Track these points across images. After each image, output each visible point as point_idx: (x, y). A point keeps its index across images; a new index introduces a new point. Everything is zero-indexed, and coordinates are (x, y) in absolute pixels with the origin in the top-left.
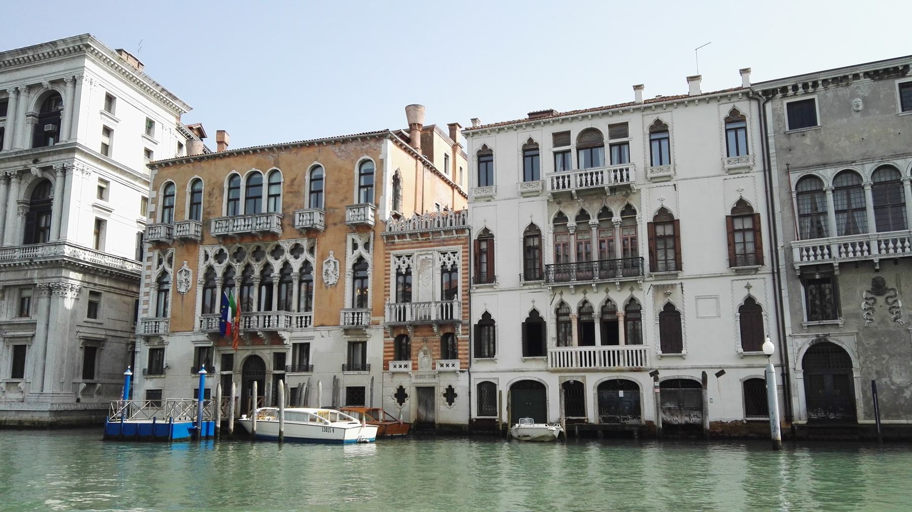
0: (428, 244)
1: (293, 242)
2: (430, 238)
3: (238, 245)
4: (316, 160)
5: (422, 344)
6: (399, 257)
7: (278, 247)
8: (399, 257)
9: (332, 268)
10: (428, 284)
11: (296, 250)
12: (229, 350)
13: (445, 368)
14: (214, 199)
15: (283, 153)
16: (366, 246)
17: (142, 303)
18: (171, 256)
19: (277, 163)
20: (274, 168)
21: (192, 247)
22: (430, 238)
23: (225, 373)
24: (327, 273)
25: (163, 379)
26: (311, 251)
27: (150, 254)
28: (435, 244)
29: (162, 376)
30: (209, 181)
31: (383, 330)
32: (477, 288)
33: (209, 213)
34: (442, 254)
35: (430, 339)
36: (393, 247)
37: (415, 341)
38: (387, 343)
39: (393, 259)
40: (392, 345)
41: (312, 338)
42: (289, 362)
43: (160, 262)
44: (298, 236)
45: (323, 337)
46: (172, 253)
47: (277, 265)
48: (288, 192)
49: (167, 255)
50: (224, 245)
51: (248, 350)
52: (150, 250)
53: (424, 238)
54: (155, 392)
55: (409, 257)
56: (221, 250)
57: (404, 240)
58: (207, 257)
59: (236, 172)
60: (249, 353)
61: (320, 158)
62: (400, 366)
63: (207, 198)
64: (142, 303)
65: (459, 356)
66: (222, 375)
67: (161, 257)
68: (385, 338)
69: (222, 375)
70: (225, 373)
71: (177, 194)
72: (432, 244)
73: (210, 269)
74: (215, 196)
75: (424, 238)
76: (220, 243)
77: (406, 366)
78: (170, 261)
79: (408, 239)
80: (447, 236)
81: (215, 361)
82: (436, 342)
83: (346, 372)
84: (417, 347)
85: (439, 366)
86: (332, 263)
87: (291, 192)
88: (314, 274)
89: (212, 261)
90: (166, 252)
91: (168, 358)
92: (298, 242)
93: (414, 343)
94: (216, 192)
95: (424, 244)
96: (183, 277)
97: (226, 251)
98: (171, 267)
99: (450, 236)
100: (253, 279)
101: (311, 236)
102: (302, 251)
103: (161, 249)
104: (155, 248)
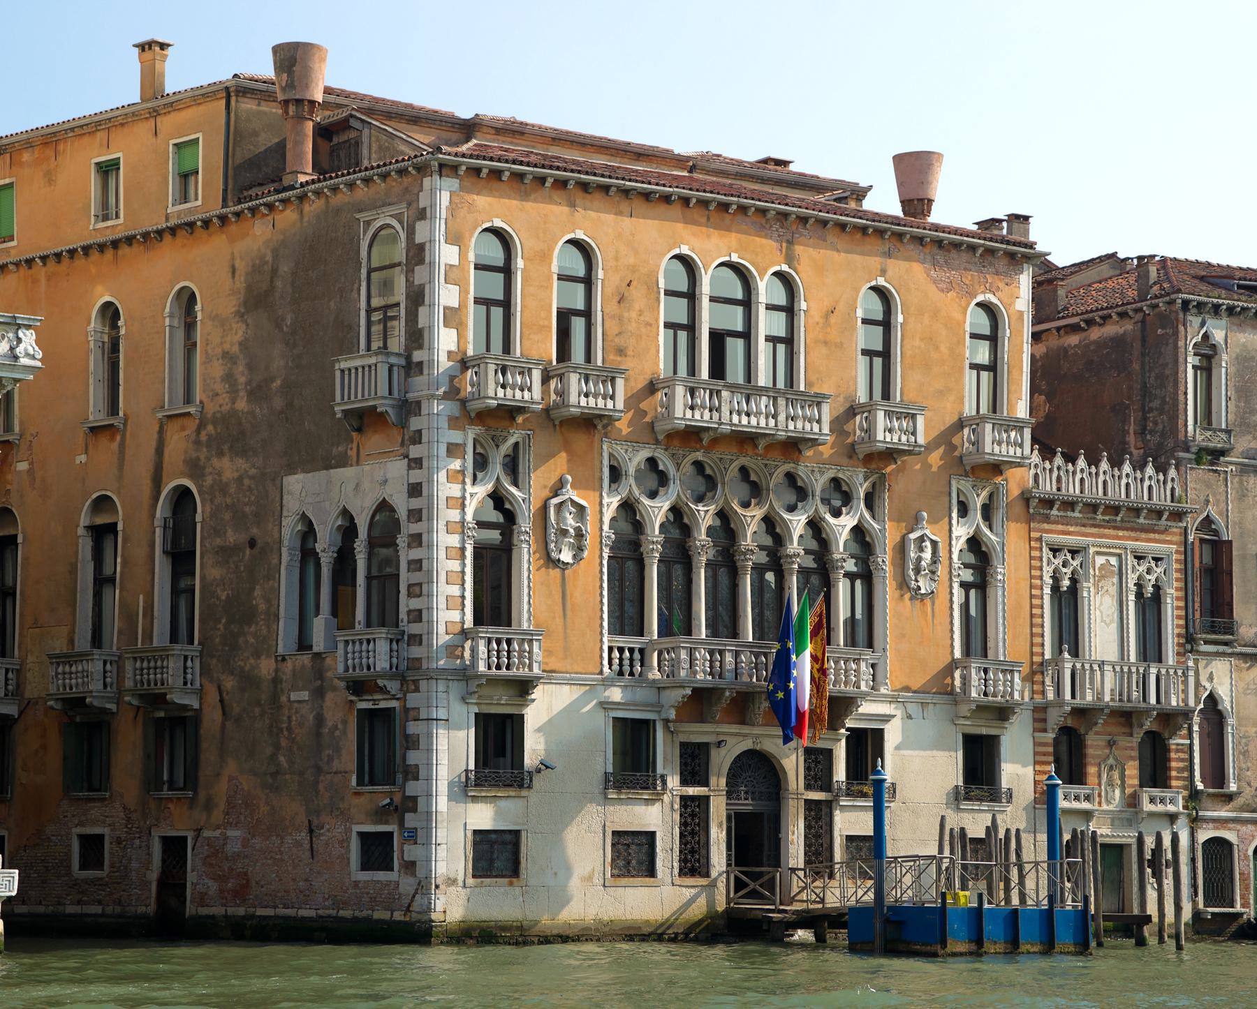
0: (1112, 532)
1: (831, 474)
2: (1119, 518)
3: (699, 456)
4: (883, 272)
5: (1107, 751)
6: (1055, 551)
7: (791, 478)
8: (1055, 551)
9: (927, 555)
10: (1112, 621)
11: (840, 495)
12: (698, 733)
13: (1160, 808)
14: (634, 315)
15: (805, 232)
16: (987, 512)
17: (443, 578)
18: (510, 452)
19: (790, 260)
20: (785, 268)
21: (580, 440)
22: (1119, 518)
23: (692, 791)
24: (918, 570)
25: (520, 803)
26: (870, 501)
27: (456, 436)
28: (1126, 533)
29: (524, 793)
30: (617, 259)
31: (1030, 713)
32: (1206, 642)
33: (621, 352)
34: (1136, 557)
35: (1123, 741)
36: (1046, 526)
37: (1094, 744)
38: (1044, 744)
39: (1046, 553)
40: (1051, 749)
41: (887, 718)
42: (840, 773)
43: (481, 463)
44: (845, 461)
45: (910, 717)
46: (516, 445)
47: (797, 523)
48: (817, 341)
49: (506, 447)
50: (666, 450)
51: (745, 736)
52: (454, 423)
53: (1107, 518)
54: (493, 836)
55: (1074, 552)
56: (652, 462)
57: (1070, 514)
58: (616, 474)
59: (688, 252)
60: (747, 745)
61: (890, 273)
62: (1077, 798)
63: (613, 307)
64: (443, 578)
65: (1174, 783)
66: (684, 799)
67: (479, 450)
68: (1035, 730)
69: (684, 799)
70: (692, 791)
71: (524, 271)
72: (1121, 533)
73: (628, 508)
74: (637, 306)
75: (1107, 518)
76: (657, 442)
77: (1088, 798)
78: (512, 467)
79: (1077, 514)
80: (1147, 522)
81: (665, 759)
82: (1132, 749)
83: (965, 805)
84: (1099, 756)
85: (1148, 800)
86: (928, 543)
87: (826, 343)
88: (885, 560)
89: (630, 485)
90: (505, 440)
91: (534, 747)
92: (840, 476)
93: (1092, 747)
94: (638, 295)
95: (1107, 531)
96: (570, 522)
97: (666, 463)
98: (516, 484)
99: (1154, 522)
100: (745, 554)
101: (874, 466)
102: (847, 498)
103: (489, 428)
104: (472, 422)
